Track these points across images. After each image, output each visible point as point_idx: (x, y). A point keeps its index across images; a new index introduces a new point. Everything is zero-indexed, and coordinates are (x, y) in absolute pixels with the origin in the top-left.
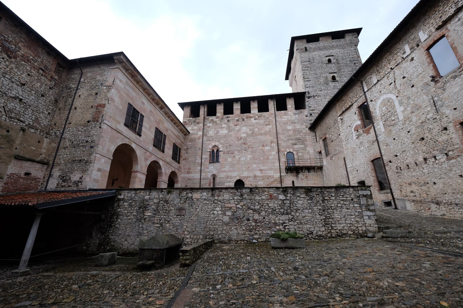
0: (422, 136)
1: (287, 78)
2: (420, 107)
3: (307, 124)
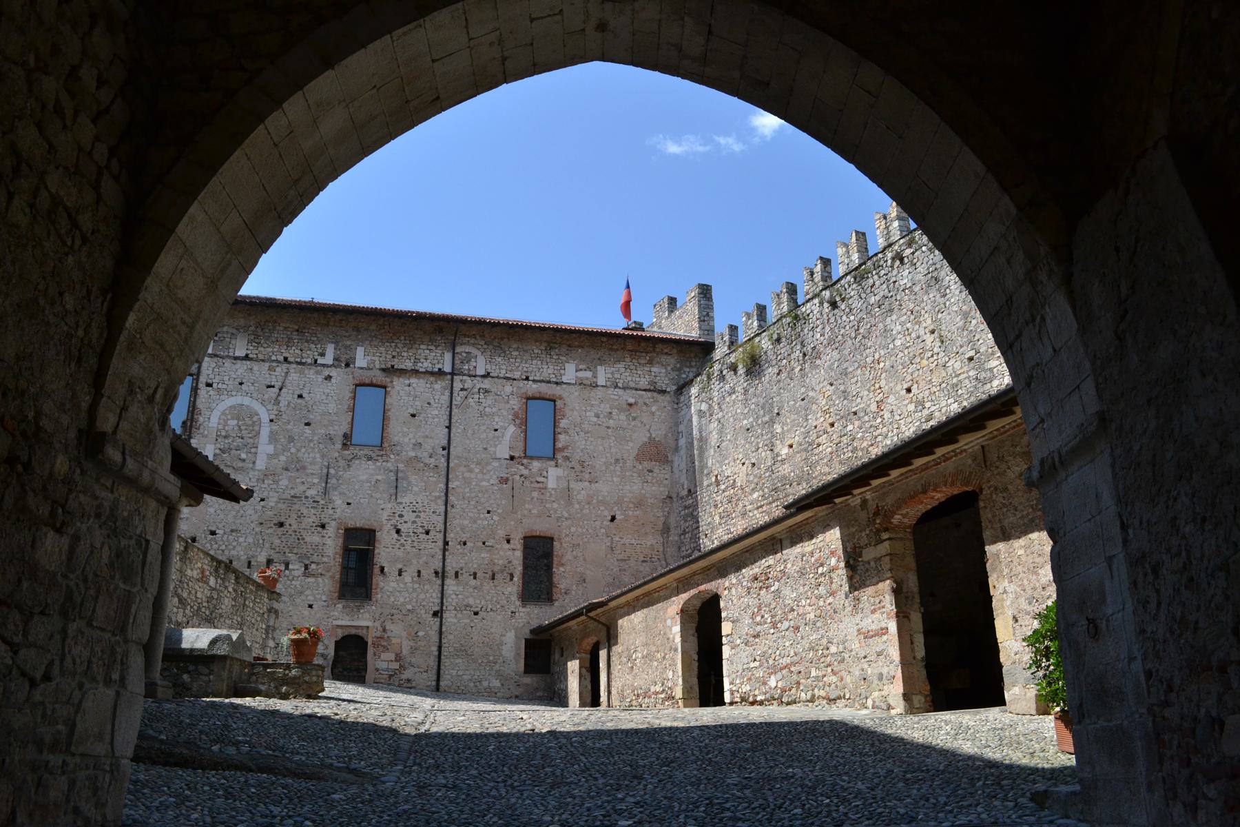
0: (282, 520)
2: (304, 468)
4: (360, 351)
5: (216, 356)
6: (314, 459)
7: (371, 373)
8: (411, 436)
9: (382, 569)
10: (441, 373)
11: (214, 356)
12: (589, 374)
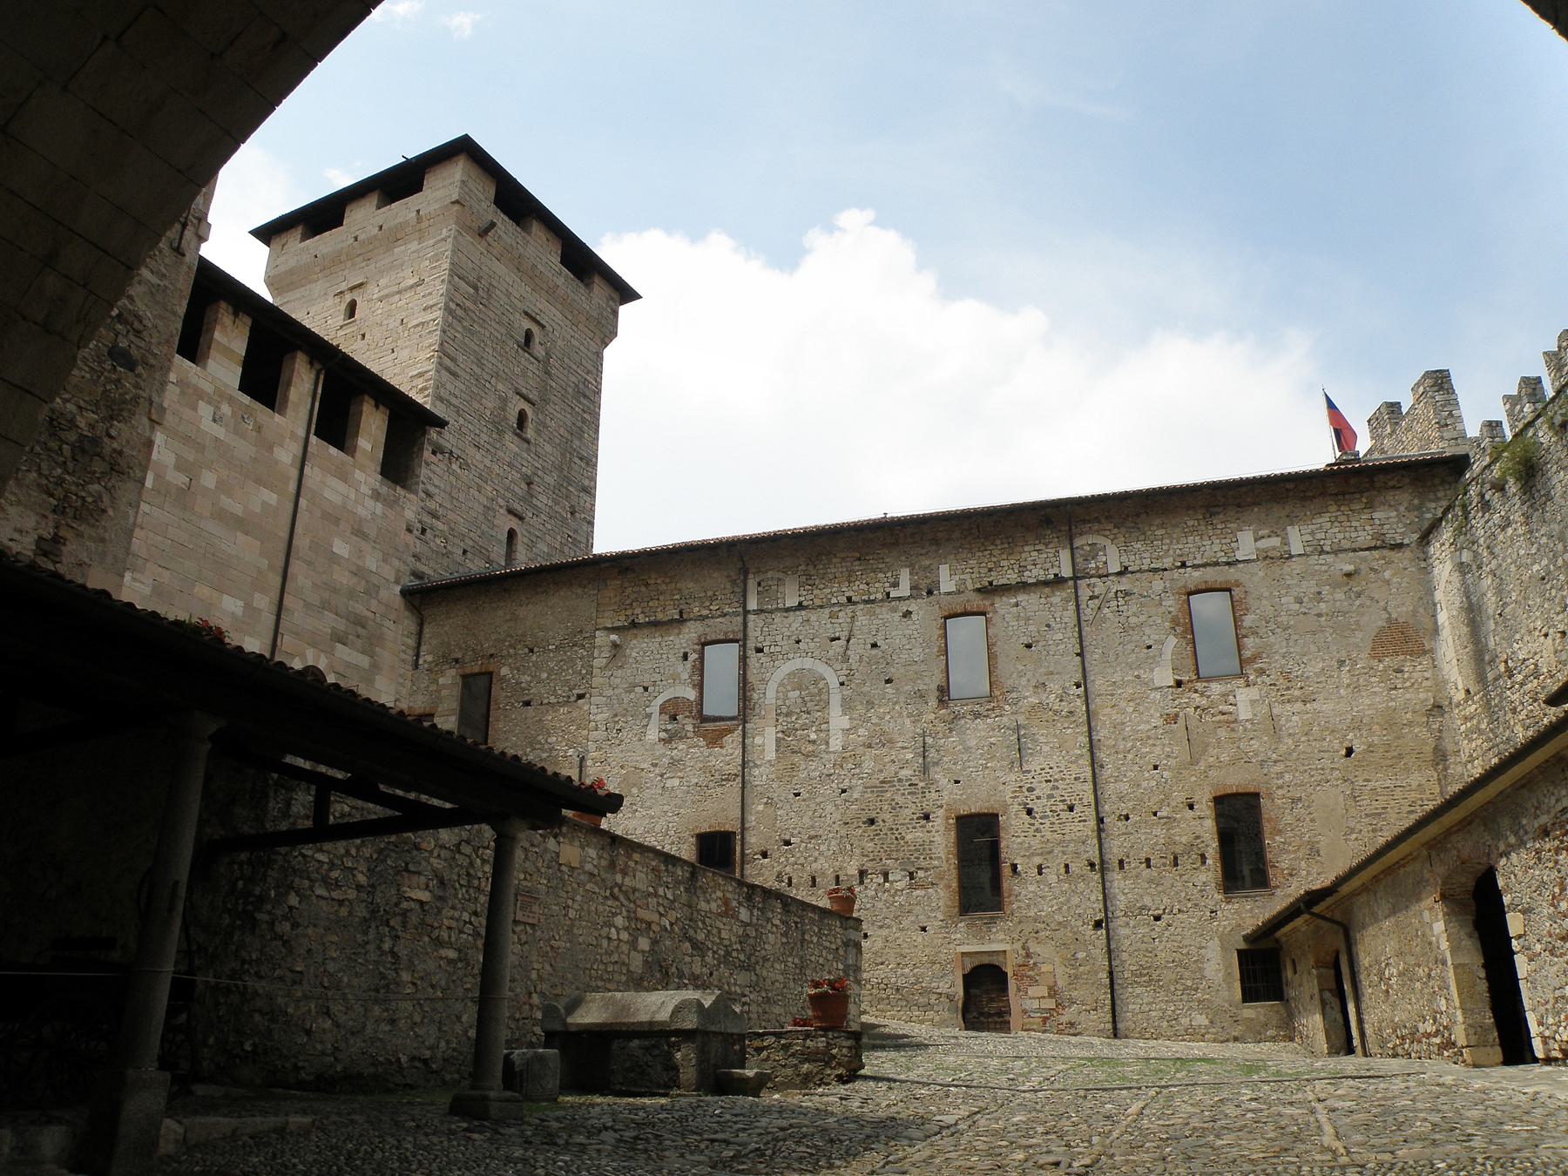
0: (873, 815)
1: (266, 233)
2: (891, 741)
3: (403, 567)
4: (944, 571)
5: (762, 611)
6: (904, 728)
7: (962, 598)
8: (1029, 674)
9: (1014, 867)
10: (1058, 581)
11: (760, 611)
12: (1275, 541)
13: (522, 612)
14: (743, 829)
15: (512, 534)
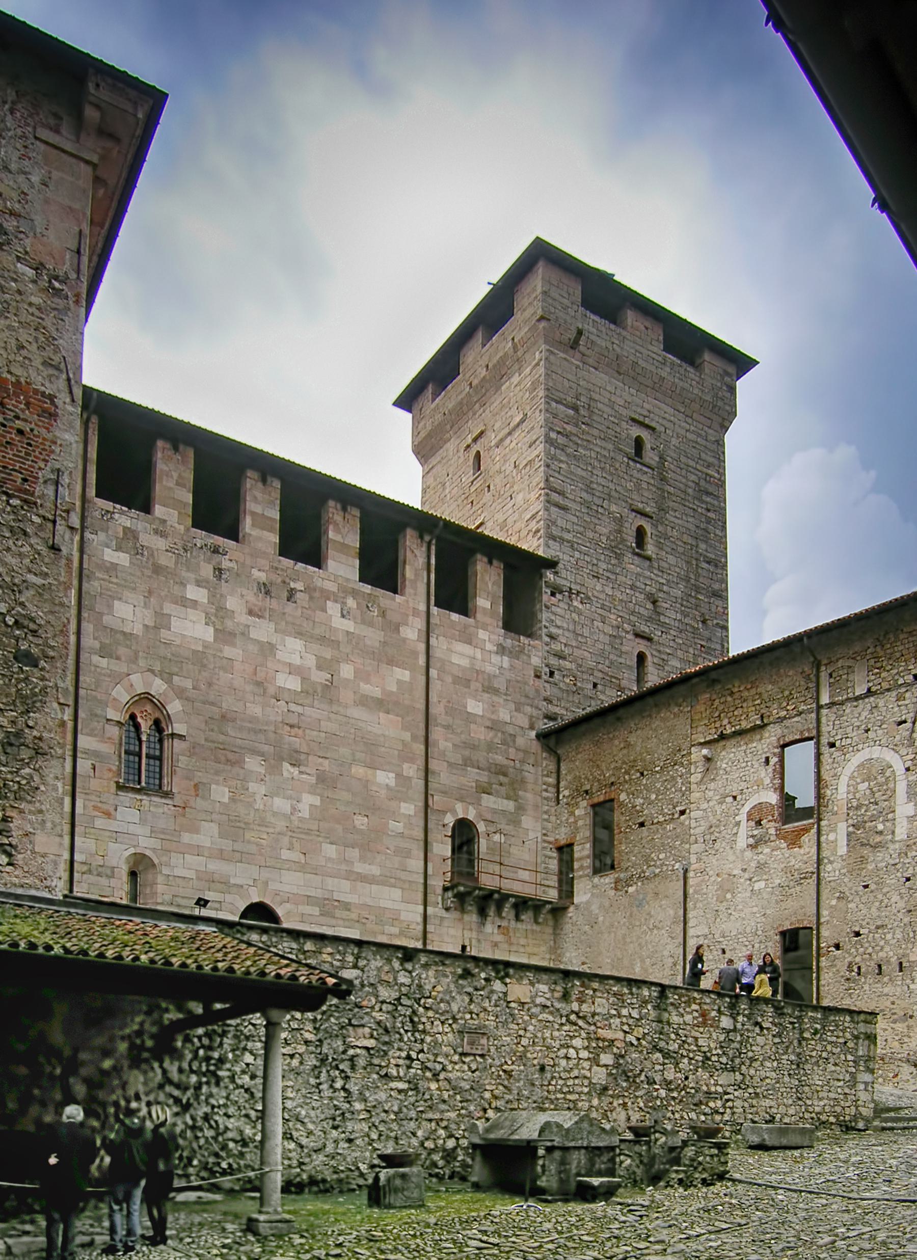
3: (535, 713)
11: (832, 704)
13: (632, 739)
14: (818, 924)
15: (641, 658)
